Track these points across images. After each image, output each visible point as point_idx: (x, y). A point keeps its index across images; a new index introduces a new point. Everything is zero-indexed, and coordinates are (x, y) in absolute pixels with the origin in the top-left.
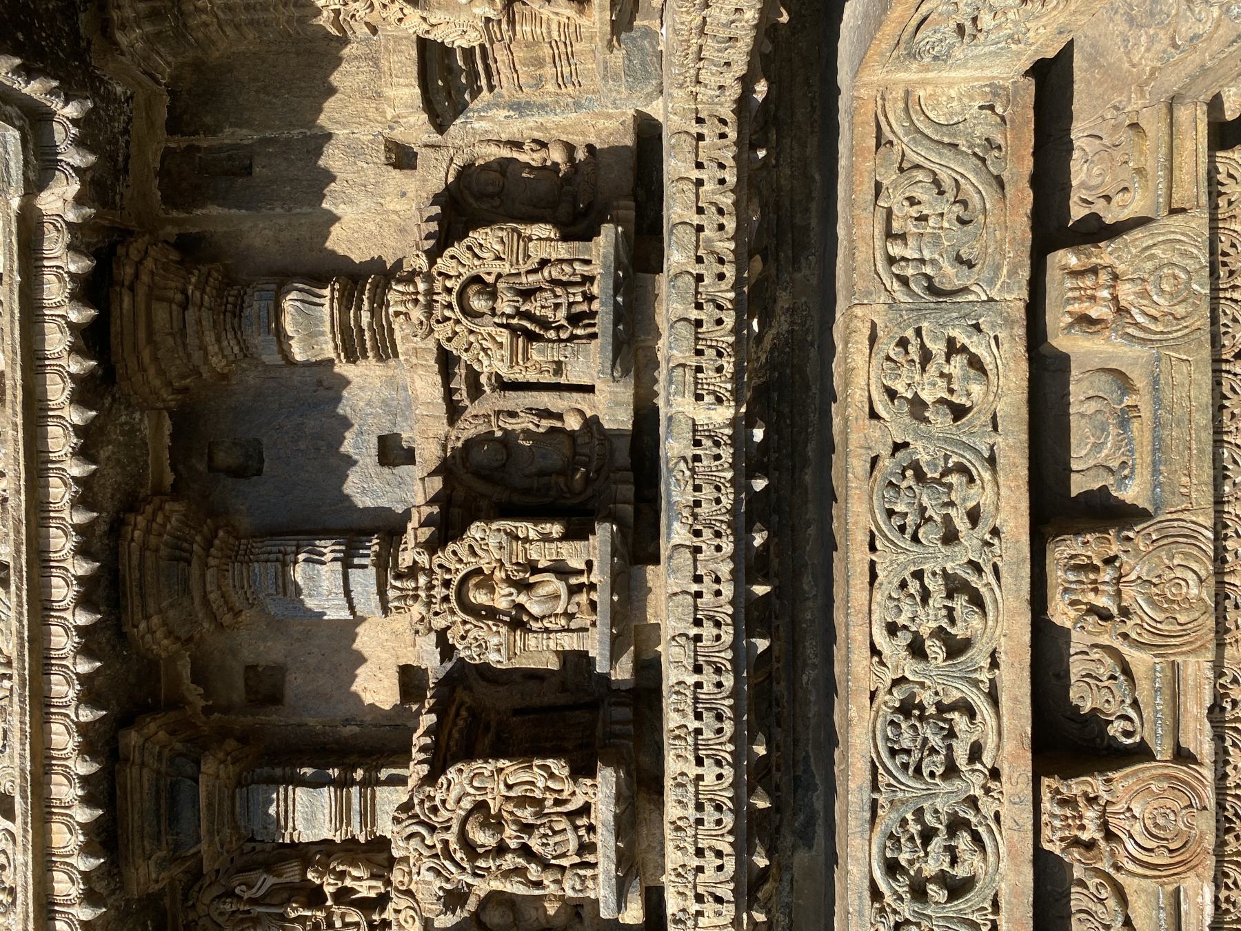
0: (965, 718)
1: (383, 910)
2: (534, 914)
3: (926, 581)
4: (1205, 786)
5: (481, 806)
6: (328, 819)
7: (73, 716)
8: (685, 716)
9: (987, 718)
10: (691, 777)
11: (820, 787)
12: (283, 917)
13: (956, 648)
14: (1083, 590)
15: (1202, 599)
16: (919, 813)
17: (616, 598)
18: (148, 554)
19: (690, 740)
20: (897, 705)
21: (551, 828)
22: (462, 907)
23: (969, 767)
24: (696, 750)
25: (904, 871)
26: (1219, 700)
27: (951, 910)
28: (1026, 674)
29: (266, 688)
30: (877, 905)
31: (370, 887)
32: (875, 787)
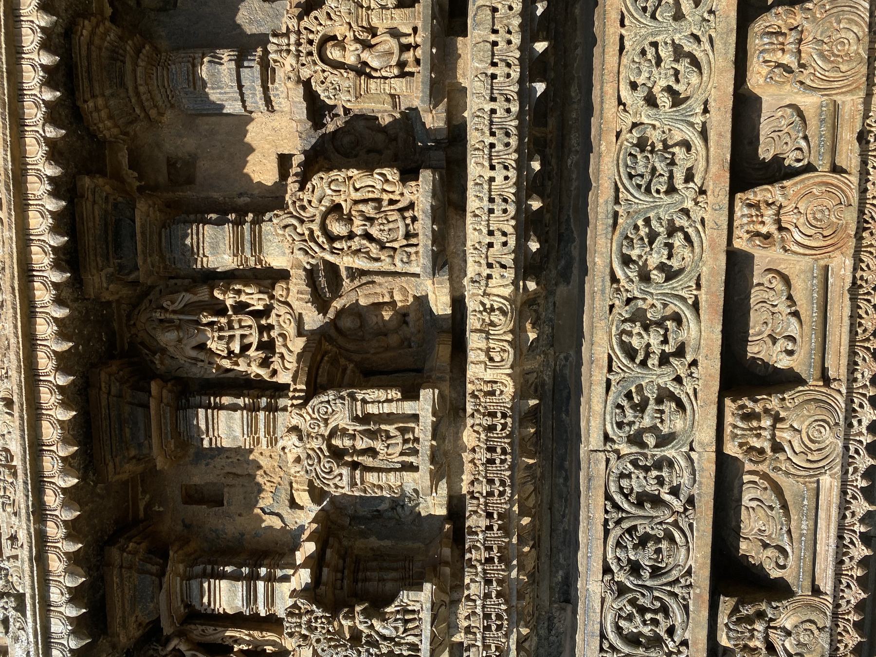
0: (684, 149)
1: (268, 317)
2: (374, 319)
3: (660, 48)
4: (851, 189)
5: (336, 208)
7: (41, 132)
8: (483, 133)
9: (699, 149)
10: (486, 178)
11: (577, 240)
12: (198, 322)
13: (677, 99)
14: (774, 50)
15: (859, 54)
16: (647, 221)
17: (434, 51)
18: (93, 48)
19: (486, 151)
20: (635, 142)
21: (386, 219)
22: (325, 315)
23: (685, 185)
24: (490, 159)
25: (634, 262)
26: (865, 134)
27: (667, 288)
28: (729, 115)
29: (181, 172)
30: (615, 286)
31: (259, 299)
32: (617, 201)
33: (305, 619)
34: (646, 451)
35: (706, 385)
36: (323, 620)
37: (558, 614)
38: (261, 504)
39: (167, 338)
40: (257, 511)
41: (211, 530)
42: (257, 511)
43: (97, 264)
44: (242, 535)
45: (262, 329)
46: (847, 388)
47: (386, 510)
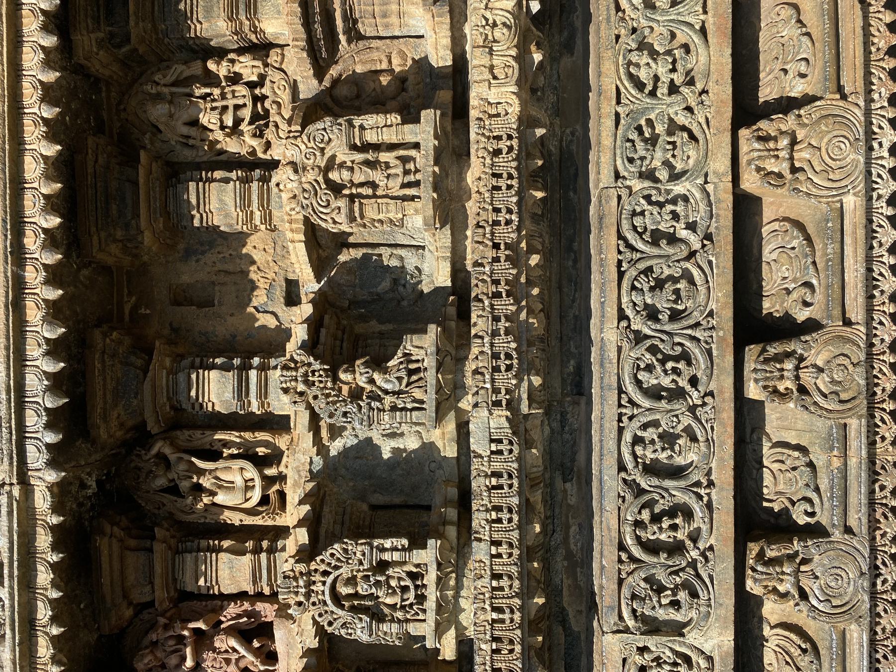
6: (222, 10)
11: (579, 9)
12: (191, 95)
33: (302, 371)
34: (659, 185)
35: (718, 112)
36: (321, 372)
37: (571, 409)
38: (255, 302)
39: (158, 112)
40: (251, 310)
41: (200, 333)
42: (251, 310)
43: (87, 26)
44: (234, 336)
45: (256, 99)
46: (865, 101)
47: (386, 292)
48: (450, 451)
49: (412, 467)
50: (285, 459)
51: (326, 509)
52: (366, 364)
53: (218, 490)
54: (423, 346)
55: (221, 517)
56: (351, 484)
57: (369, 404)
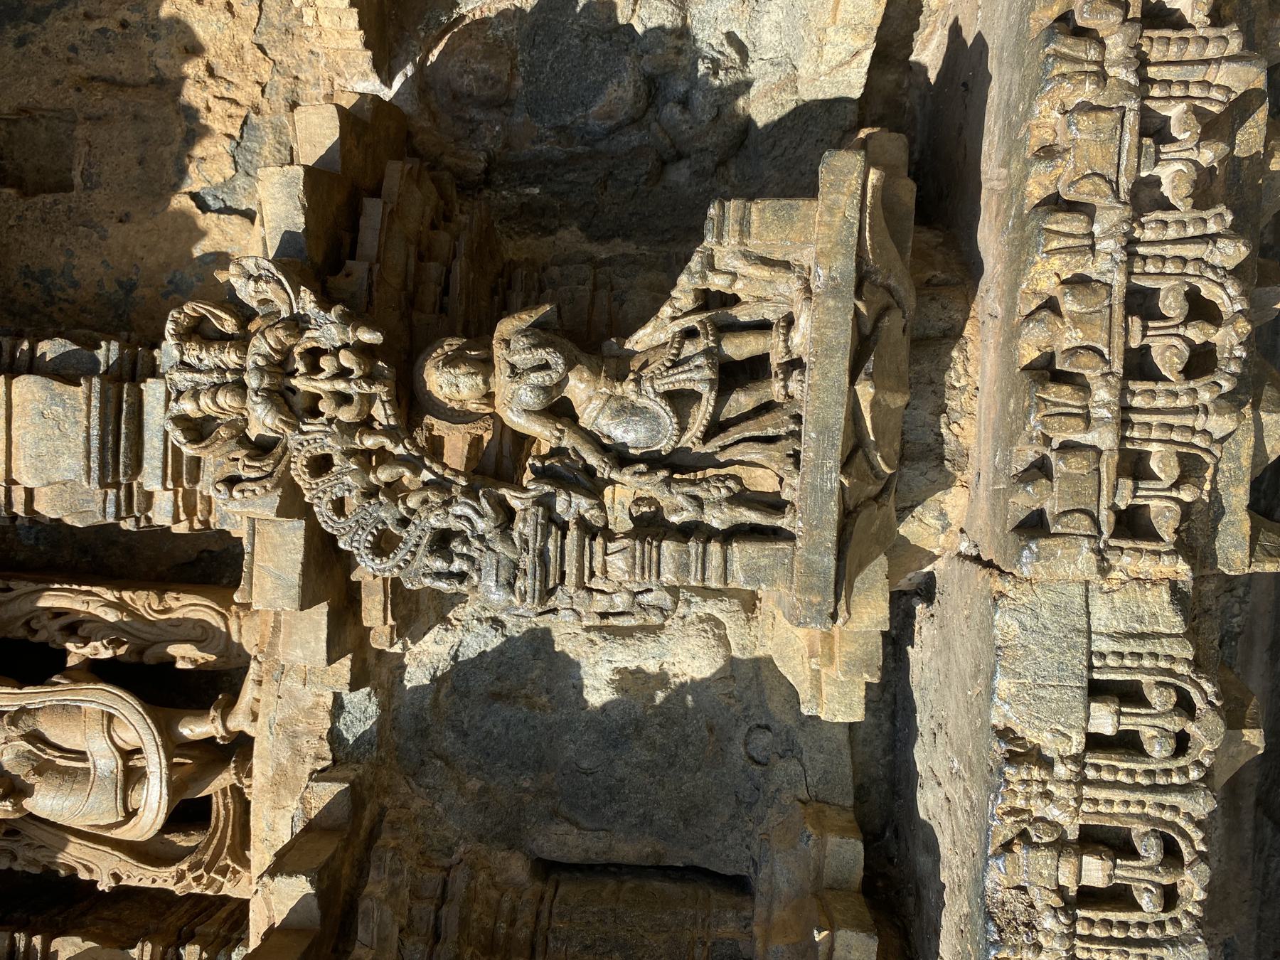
33: (261, 346)
36: (347, 360)
38: (195, 182)
40: (180, 201)
41: (26, 272)
44: (128, 287)
48: (838, 700)
49: (685, 740)
50: (248, 692)
51: (376, 887)
52: (541, 334)
53: (32, 779)
54: (782, 266)
55: (62, 858)
56: (474, 784)
57: (545, 502)
